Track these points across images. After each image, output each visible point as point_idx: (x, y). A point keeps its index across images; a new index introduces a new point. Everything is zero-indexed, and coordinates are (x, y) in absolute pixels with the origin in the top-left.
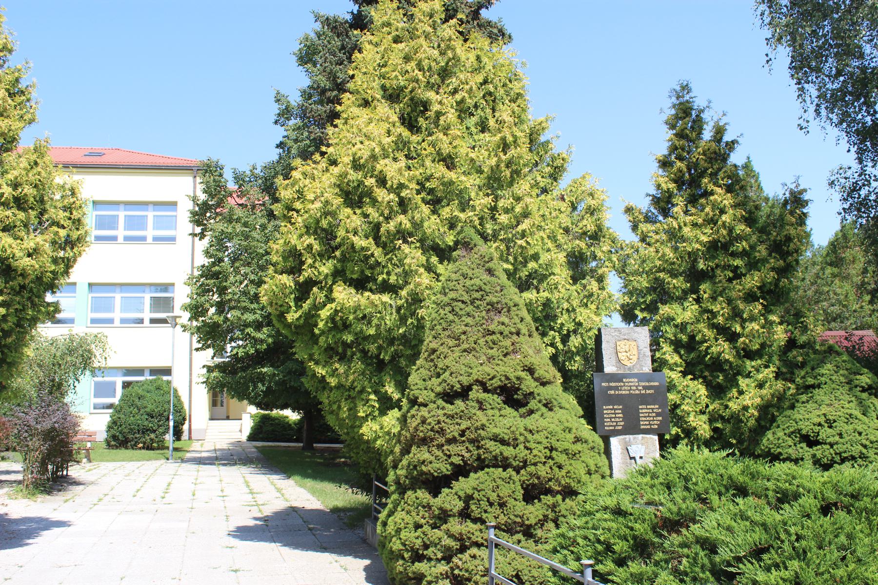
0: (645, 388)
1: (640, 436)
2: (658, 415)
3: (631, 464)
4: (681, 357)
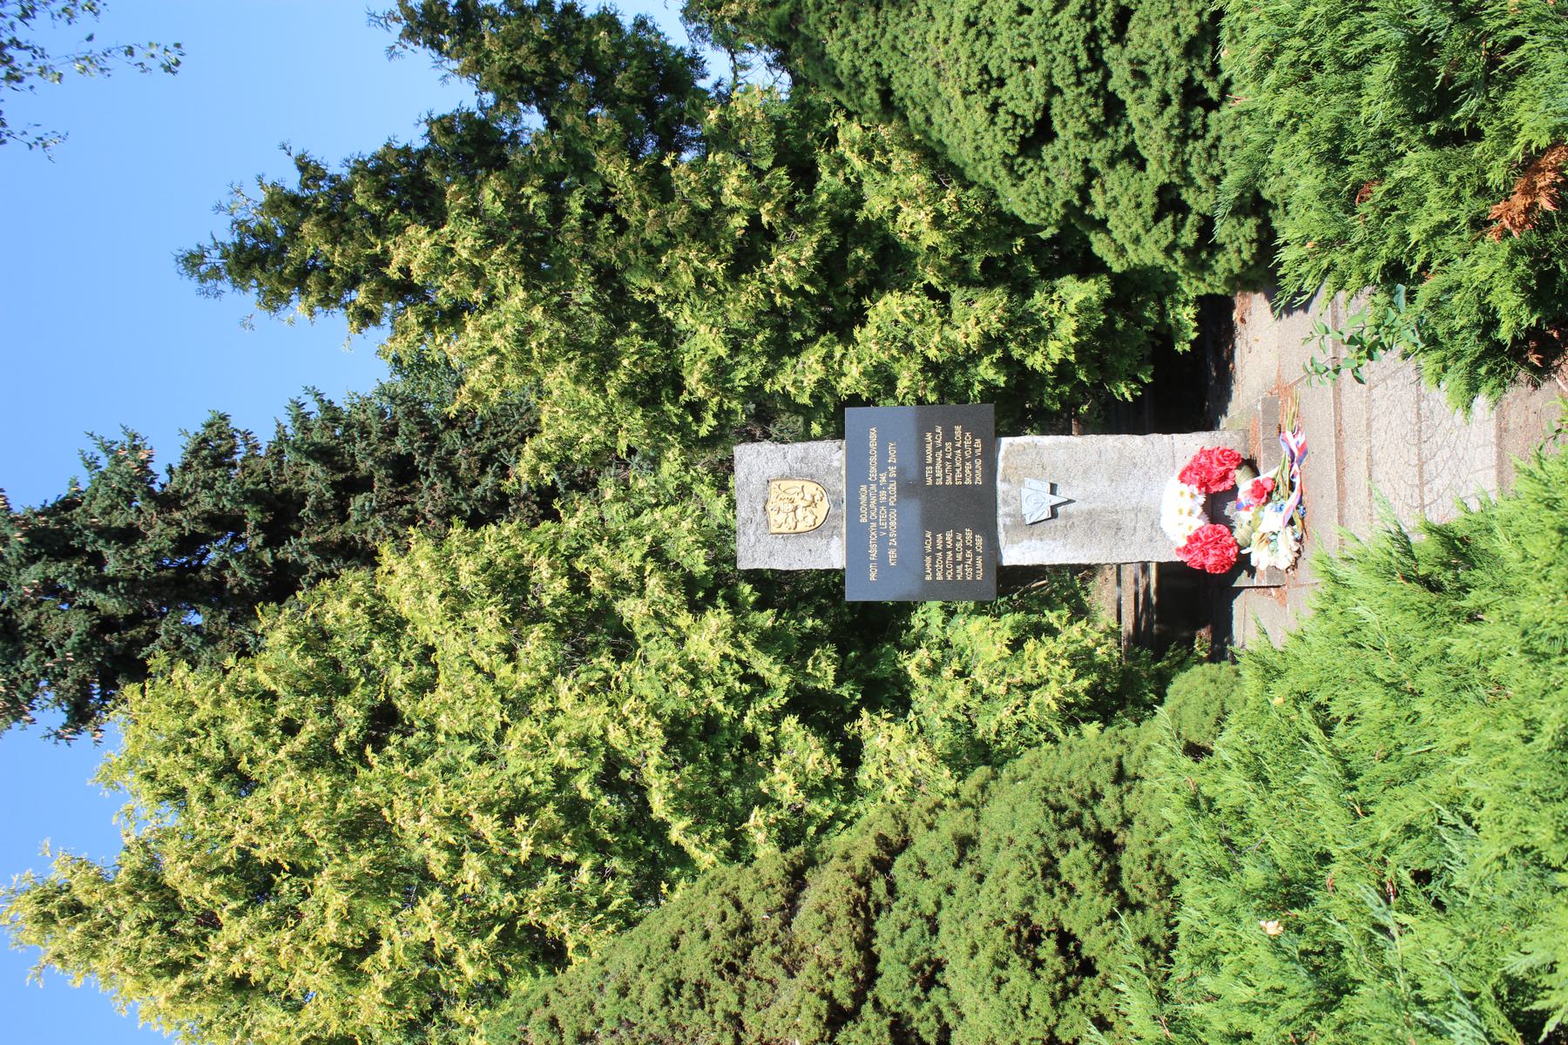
0: (882, 467)
1: (1001, 486)
2: (949, 436)
3: (1068, 516)
4: (811, 341)
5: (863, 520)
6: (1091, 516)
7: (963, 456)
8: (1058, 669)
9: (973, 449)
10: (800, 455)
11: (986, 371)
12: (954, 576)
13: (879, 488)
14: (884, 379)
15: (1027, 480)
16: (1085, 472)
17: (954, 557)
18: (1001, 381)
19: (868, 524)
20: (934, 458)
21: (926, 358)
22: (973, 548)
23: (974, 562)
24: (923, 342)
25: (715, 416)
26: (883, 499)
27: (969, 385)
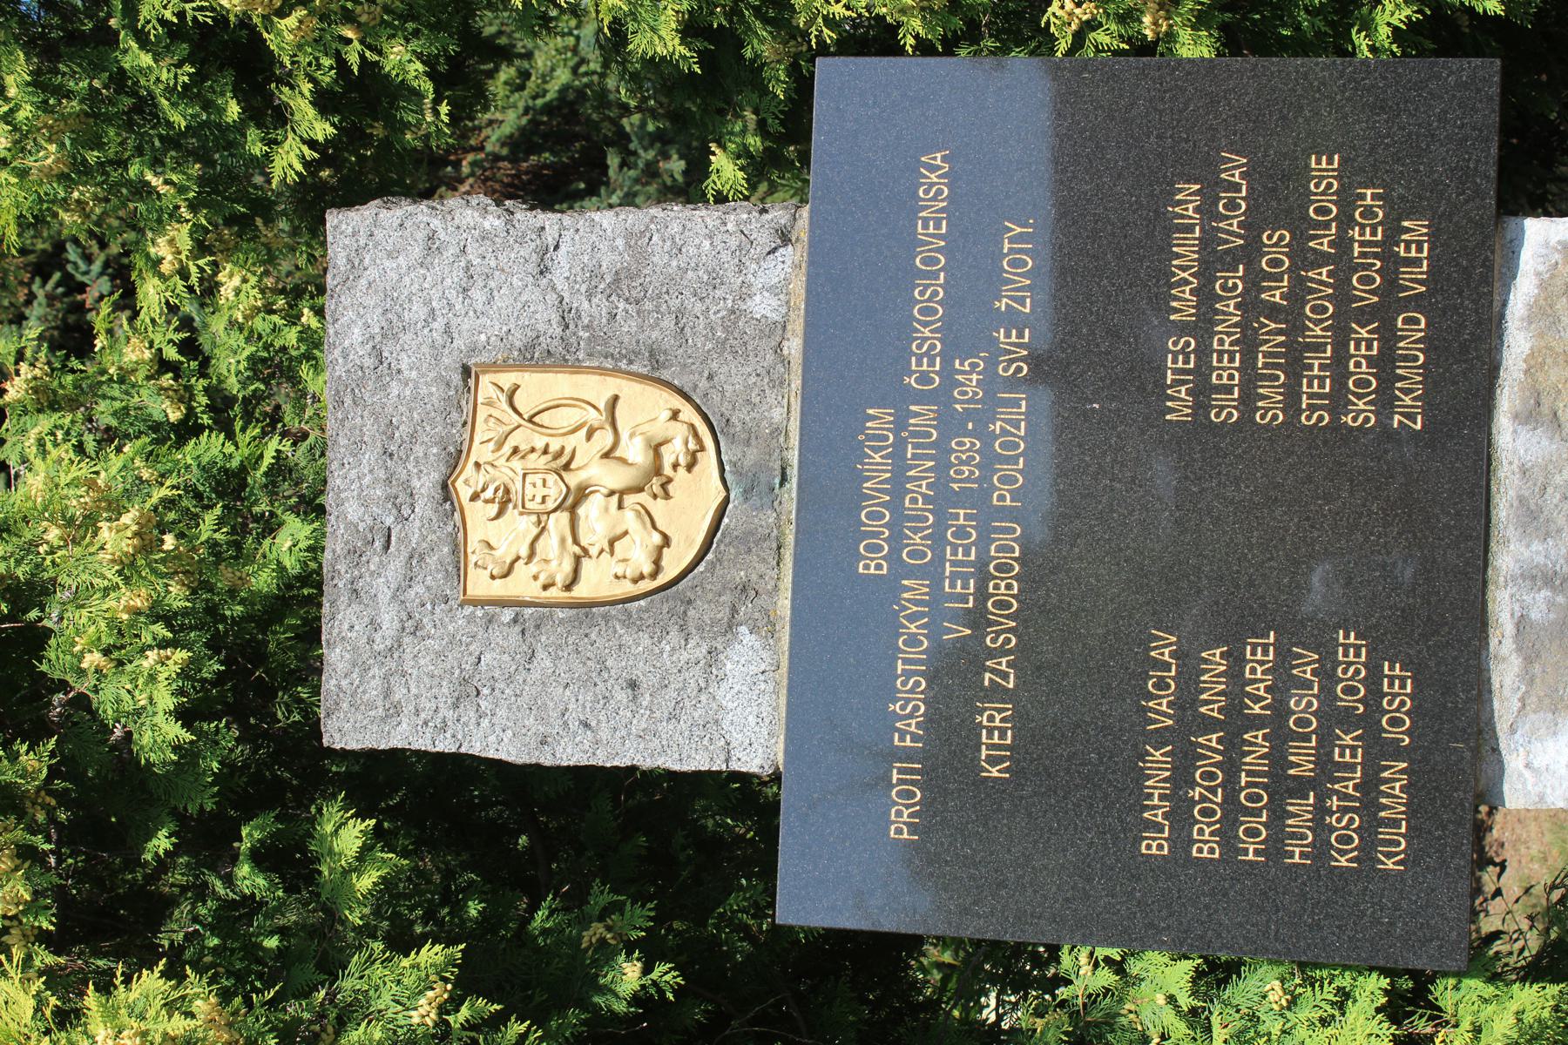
1: (1514, 442)
2: (1280, 198)
5: (872, 566)
7: (1342, 295)
10: (608, 261)
12: (1275, 847)
13: (950, 424)
17: (1277, 759)
19: (889, 587)
20: (1206, 296)
23: (1370, 785)
25: (324, 102)
26: (964, 474)
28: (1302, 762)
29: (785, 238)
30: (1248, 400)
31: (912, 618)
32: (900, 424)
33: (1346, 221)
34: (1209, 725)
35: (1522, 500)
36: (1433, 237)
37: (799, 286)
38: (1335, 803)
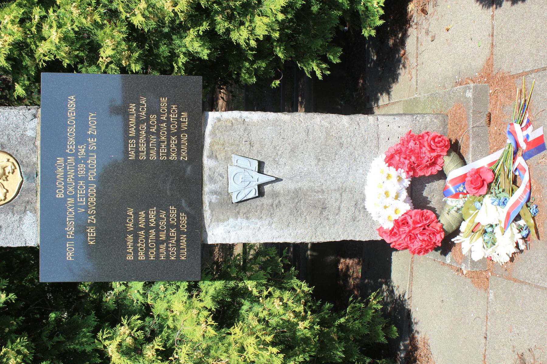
0: (81, 139)
1: (207, 163)
3: (275, 195)
5: (60, 195)
6: (297, 195)
7: (169, 130)
8: (266, 354)
9: (180, 123)
11: (192, 43)
12: (157, 256)
13: (78, 161)
14: (86, 47)
15: (235, 158)
16: (293, 151)
17: (157, 236)
18: (205, 54)
19: (64, 200)
20: (138, 131)
21: (131, 26)
22: (177, 227)
23: (178, 241)
24: (129, 9)
26: (82, 173)
27: (173, 56)
28: (163, 237)
29: (35, 116)
30: (148, 154)
31: (70, 208)
32: (65, 161)
33: (169, 113)
34: (141, 229)
35: (209, 175)
36: (189, 116)
37: (39, 128)
38: (170, 245)
